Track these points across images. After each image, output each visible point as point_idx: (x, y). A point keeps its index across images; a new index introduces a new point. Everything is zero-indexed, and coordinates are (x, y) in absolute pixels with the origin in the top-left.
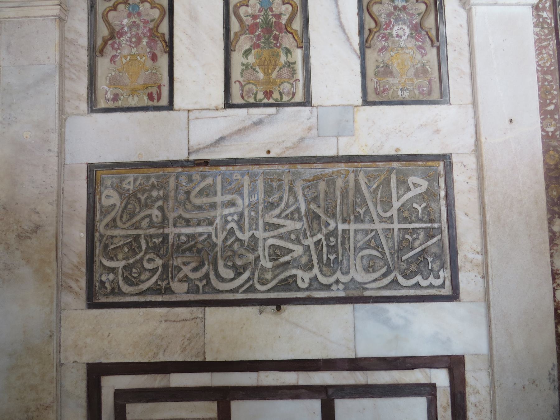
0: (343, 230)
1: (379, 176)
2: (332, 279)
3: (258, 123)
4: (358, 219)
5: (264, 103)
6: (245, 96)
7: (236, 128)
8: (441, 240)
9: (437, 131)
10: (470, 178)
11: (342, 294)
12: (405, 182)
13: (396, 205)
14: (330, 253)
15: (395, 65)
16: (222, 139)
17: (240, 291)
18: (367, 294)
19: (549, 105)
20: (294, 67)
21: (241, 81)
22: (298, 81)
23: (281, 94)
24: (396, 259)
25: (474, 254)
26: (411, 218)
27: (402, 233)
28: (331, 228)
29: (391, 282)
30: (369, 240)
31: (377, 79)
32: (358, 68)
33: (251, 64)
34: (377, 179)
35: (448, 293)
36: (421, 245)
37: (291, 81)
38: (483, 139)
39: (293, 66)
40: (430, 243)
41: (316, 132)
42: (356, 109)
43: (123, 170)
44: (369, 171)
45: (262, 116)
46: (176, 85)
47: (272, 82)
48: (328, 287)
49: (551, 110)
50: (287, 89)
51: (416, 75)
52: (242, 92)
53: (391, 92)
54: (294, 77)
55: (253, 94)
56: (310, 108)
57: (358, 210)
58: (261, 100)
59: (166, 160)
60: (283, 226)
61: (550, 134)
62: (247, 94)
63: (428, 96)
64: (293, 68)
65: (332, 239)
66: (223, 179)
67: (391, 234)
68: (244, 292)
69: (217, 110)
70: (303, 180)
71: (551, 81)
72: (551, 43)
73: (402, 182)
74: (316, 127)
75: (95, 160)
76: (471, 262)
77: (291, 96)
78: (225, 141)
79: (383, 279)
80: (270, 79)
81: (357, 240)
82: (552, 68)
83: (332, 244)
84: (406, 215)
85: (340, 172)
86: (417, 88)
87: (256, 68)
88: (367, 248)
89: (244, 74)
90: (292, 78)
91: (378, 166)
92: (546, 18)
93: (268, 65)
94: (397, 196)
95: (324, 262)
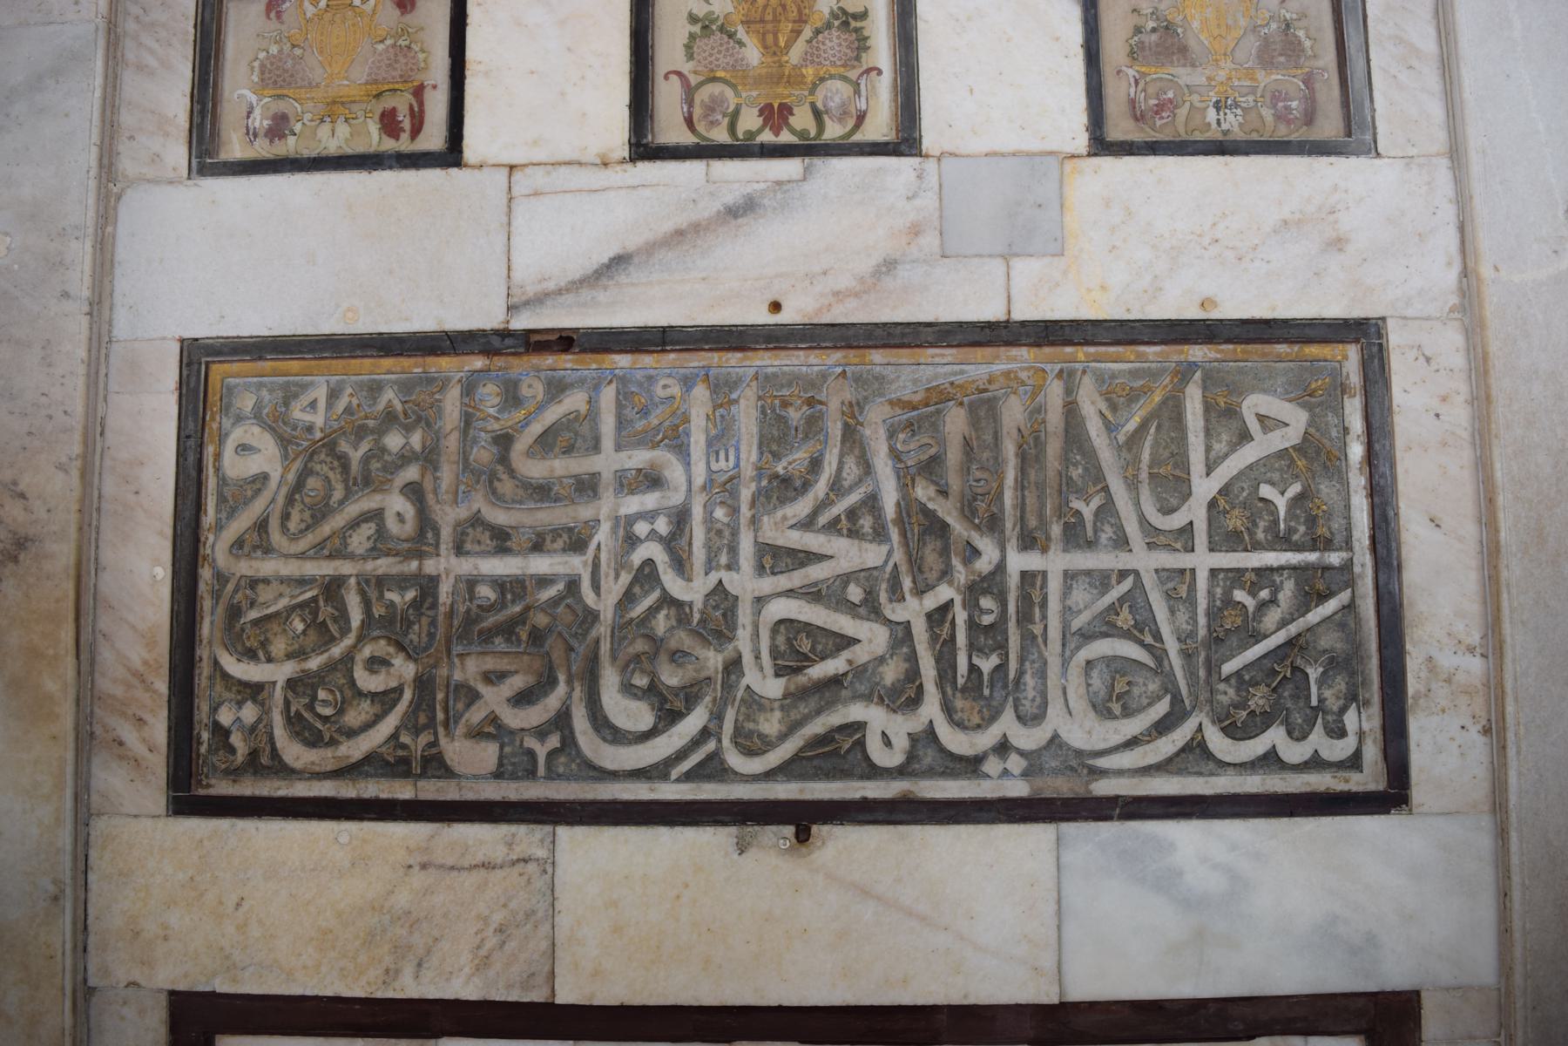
0: (1024, 574)
1: (1146, 391)
2: (985, 740)
3: (743, 210)
4: (1075, 536)
5: (762, 145)
6: (699, 121)
7: (668, 226)
8: (1350, 607)
9: (1338, 243)
11: (1018, 789)
12: (1232, 413)
13: (1204, 487)
14: (980, 650)
15: (1196, 25)
16: (619, 261)
17: (675, 774)
18: (1103, 788)
20: (862, 28)
21: (686, 73)
22: (876, 72)
23: (817, 115)
24: (1202, 673)
25: (1459, 652)
26: (1251, 533)
27: (1221, 583)
28: (984, 565)
29: (1183, 750)
30: (1113, 609)
31: (1137, 68)
32: (1074, 33)
33: (722, 17)
34: (1138, 400)
35: (1372, 787)
36: (1283, 624)
37: (853, 75)
38: (1486, 271)
39: (859, 24)
40: (1314, 616)
41: (937, 242)
42: (1069, 165)
43: (296, 362)
44: (1113, 376)
45: (756, 186)
46: (474, 86)
47: (789, 76)
48: (971, 765)
50: (837, 100)
51: (1266, 59)
52: (689, 109)
53: (1183, 112)
54: (863, 60)
55: (724, 115)
56: (917, 160)
57: (1077, 504)
58: (751, 135)
59: (432, 329)
60: (821, 558)
62: (706, 116)
63: (1305, 128)
64: (857, 30)
65: (986, 602)
66: (621, 397)
67: (1185, 587)
68: (688, 777)
69: (605, 165)
70: (891, 403)
73: (1223, 414)
74: (937, 223)
75: (205, 328)
76: (1448, 681)
77: (851, 123)
78: (631, 268)
79: (1156, 738)
80: (781, 66)
81: (1070, 608)
83: (987, 620)
84: (1235, 521)
85: (1016, 378)
86: (1268, 100)
87: (736, 31)
88: (1106, 635)
89: (695, 49)
90: (856, 63)
91: (1141, 358)
93: (776, 20)
94: (1207, 458)
95: (961, 681)
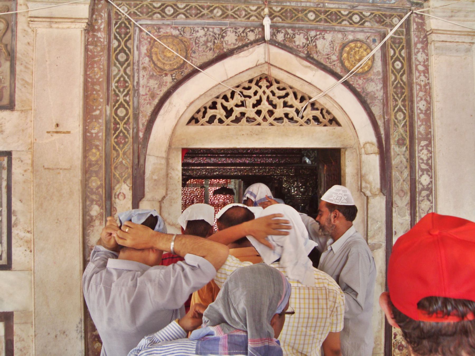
10: (25, 171)
19: (95, 111)
35: (4, 264)
61: (94, 135)
71: (99, 91)
72: (102, 58)
82: (101, 80)
92: (100, 38)
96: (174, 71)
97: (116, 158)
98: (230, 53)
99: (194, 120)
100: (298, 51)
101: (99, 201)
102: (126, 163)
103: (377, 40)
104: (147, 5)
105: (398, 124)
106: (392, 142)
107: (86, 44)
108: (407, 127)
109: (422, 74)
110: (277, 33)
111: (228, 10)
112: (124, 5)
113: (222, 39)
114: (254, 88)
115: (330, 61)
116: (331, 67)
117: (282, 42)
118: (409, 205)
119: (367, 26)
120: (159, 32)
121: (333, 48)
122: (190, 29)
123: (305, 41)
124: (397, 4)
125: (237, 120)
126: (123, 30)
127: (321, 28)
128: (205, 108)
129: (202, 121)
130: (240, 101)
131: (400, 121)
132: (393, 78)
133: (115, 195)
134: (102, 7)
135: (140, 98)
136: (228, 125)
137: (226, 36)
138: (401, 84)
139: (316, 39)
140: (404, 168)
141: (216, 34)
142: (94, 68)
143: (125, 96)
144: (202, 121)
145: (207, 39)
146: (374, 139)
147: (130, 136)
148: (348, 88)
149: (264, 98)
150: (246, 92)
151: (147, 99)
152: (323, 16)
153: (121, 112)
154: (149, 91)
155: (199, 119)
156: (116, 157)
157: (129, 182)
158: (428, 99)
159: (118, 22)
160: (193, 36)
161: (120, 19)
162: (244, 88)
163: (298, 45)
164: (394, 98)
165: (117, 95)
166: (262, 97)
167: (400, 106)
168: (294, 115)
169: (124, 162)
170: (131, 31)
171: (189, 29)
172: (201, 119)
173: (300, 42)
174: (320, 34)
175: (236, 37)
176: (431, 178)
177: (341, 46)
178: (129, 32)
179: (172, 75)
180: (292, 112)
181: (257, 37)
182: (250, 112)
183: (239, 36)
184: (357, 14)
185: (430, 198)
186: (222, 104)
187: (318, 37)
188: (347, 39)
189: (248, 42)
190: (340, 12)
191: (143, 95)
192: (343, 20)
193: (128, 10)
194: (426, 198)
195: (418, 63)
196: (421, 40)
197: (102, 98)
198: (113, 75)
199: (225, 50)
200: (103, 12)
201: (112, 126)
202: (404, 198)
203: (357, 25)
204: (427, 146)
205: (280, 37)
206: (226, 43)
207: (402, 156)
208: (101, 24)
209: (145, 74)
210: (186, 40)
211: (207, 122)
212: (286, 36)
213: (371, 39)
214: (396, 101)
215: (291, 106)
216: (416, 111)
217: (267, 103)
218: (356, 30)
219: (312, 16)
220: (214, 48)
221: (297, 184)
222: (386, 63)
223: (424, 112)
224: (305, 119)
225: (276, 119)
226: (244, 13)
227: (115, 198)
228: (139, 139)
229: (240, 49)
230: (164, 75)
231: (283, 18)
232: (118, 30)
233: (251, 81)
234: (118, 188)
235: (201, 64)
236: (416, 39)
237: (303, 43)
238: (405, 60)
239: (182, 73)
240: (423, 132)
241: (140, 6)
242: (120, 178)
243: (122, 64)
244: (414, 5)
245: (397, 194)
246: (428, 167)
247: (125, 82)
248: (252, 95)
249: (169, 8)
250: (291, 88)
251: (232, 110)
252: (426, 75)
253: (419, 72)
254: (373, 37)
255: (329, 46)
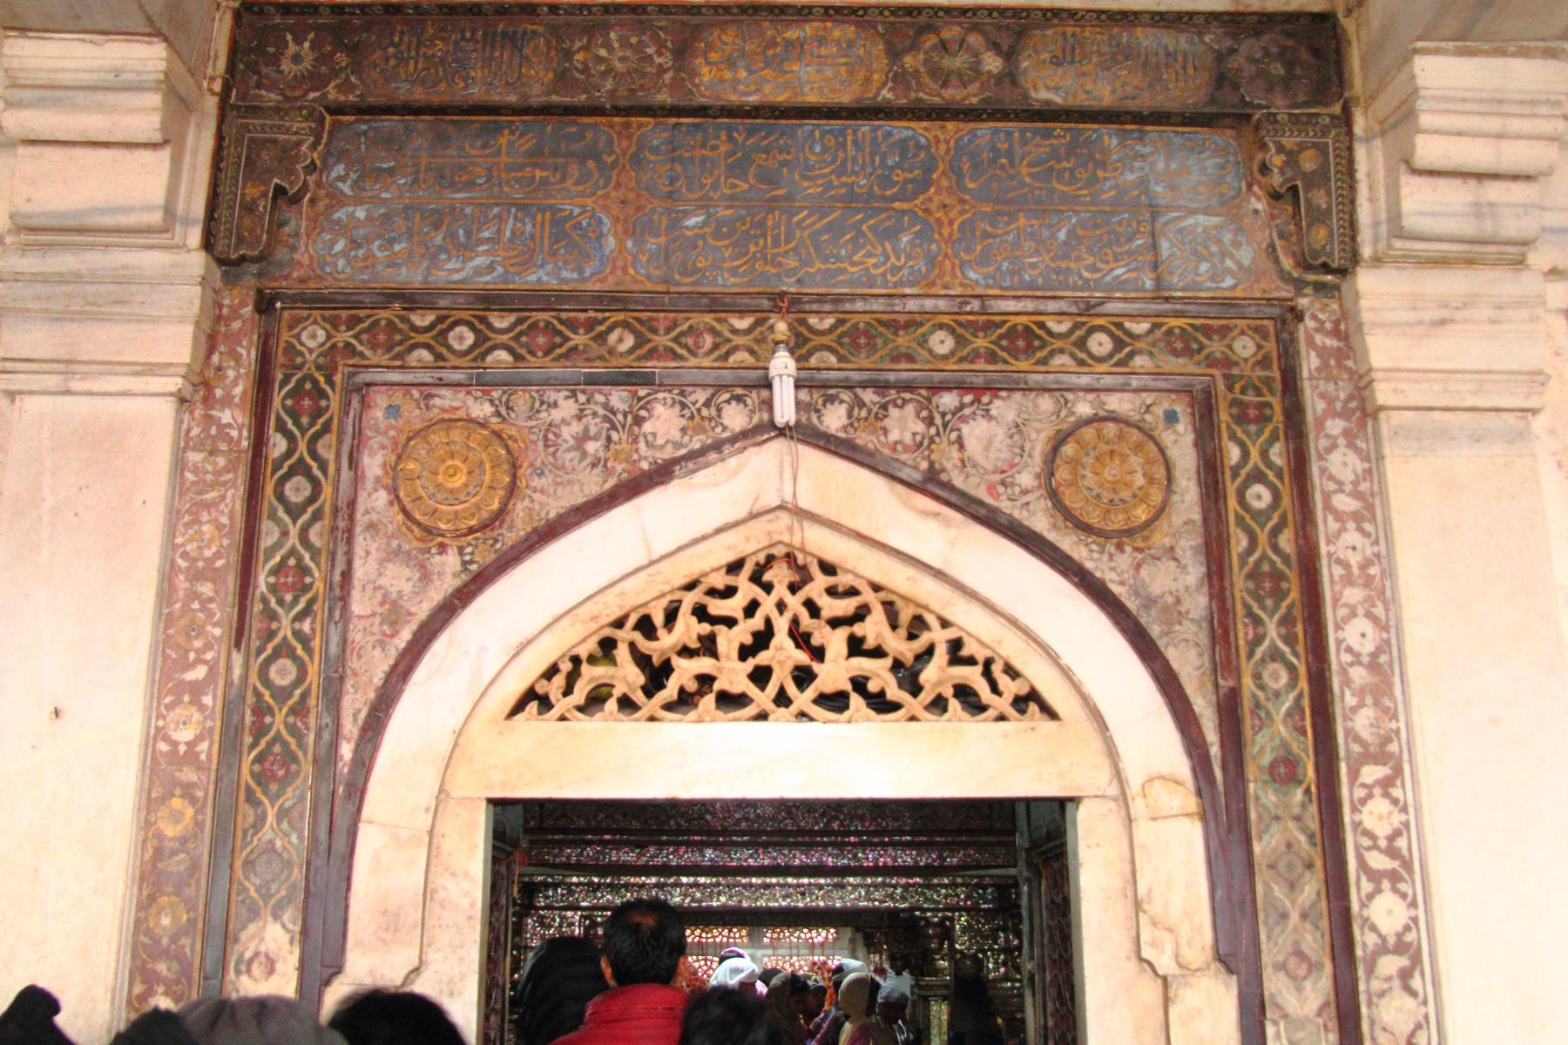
19: (193, 666)
49: (197, 681)
61: (182, 749)
71: (211, 600)
72: (230, 493)
82: (220, 563)
92: (229, 426)
96: (470, 537)
97: (251, 832)
98: (661, 474)
99: (534, 699)
100: (897, 460)
101: (178, 982)
102: (284, 848)
103: (1179, 415)
104: (390, 323)
105: (1270, 706)
106: (1251, 771)
107: (182, 445)
108: (1303, 719)
109: (1351, 525)
110: (824, 405)
111: (654, 331)
112: (315, 322)
113: (636, 429)
114: (747, 591)
115: (1009, 491)
116: (1016, 514)
117: (842, 435)
118: (1332, 1011)
119: (1142, 367)
120: (428, 407)
121: (1022, 448)
122: (531, 397)
123: (920, 427)
124: (1244, 290)
125: (685, 701)
126: (307, 402)
127: (975, 380)
128: (576, 660)
129: (562, 705)
130: (695, 636)
131: (1277, 694)
132: (1244, 543)
133: (239, 962)
134: (240, 329)
135: (351, 627)
136: (652, 719)
137: (651, 416)
138: (1272, 562)
139: (964, 420)
140: (1300, 869)
141: (614, 413)
142: (200, 523)
143: (300, 617)
144: (562, 705)
145: (586, 429)
146: (1181, 765)
147: (305, 754)
148: (1077, 585)
149: (781, 625)
150: (717, 607)
151: (376, 628)
152: (981, 342)
153: (283, 674)
154: (382, 604)
155: (553, 699)
156: (254, 826)
157: (291, 916)
158: (1379, 611)
159: (294, 375)
160: (538, 419)
161: (300, 367)
162: (712, 592)
163: (896, 443)
164: (1250, 613)
165: (273, 616)
166: (775, 623)
167: (1273, 641)
168: (886, 682)
169: (279, 844)
170: (332, 404)
171: (527, 396)
172: (558, 700)
173: (902, 431)
174: (977, 400)
175: (683, 422)
176: (1413, 904)
177: (1049, 439)
178: (328, 407)
179: (461, 550)
180: (880, 675)
181: (756, 420)
182: (733, 675)
183: (692, 417)
184: (1101, 328)
185: (1416, 983)
186: (632, 646)
187: (967, 411)
188: (1073, 413)
189: (725, 435)
190: (1042, 325)
191: (360, 617)
192: (1052, 354)
193: (329, 337)
194: (1396, 983)
195: (1332, 486)
196: (1338, 406)
197: (215, 625)
198: (262, 549)
199: (645, 465)
200: (245, 343)
201: (249, 718)
202: (1308, 984)
203: (1104, 367)
204: (1386, 784)
205: (834, 419)
206: (647, 442)
207: (1291, 825)
208: (235, 383)
209: (373, 547)
210: (513, 432)
211: (580, 709)
212: (856, 410)
213: (1159, 411)
214: (1257, 621)
215: (878, 653)
216: (1336, 658)
217: (790, 644)
218: (1102, 381)
219: (942, 342)
220: (606, 461)
221: (1007, 939)
222: (1216, 490)
223: (1366, 659)
224: (926, 696)
225: (824, 700)
226: (708, 341)
227: (238, 972)
228: (340, 764)
229: (696, 458)
230: (434, 551)
231: (842, 351)
232: (289, 402)
233: (734, 567)
234: (252, 938)
235: (562, 511)
236: (1321, 405)
237: (914, 434)
238: (1286, 479)
239: (496, 541)
240: (1365, 734)
241: (366, 325)
242: (261, 903)
243: (294, 511)
244: (1306, 291)
245: (1281, 967)
246: (1395, 864)
247: (303, 570)
248: (739, 615)
249: (462, 330)
250: (877, 588)
251: (666, 669)
252: (1368, 527)
253: (1339, 516)
254: (1166, 405)
255: (1008, 441)
